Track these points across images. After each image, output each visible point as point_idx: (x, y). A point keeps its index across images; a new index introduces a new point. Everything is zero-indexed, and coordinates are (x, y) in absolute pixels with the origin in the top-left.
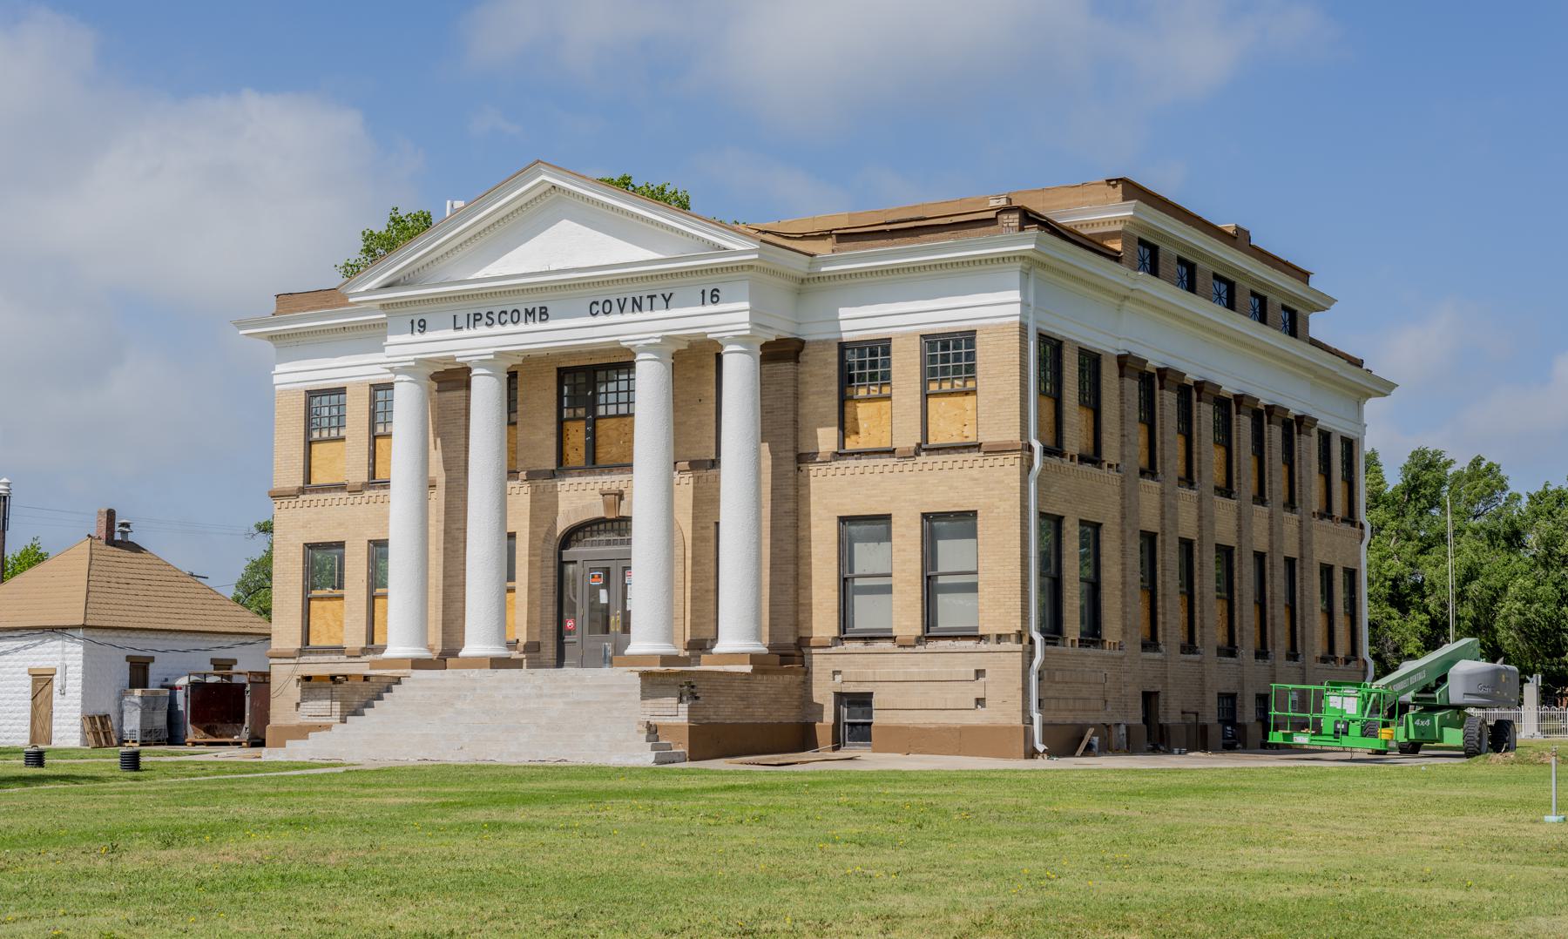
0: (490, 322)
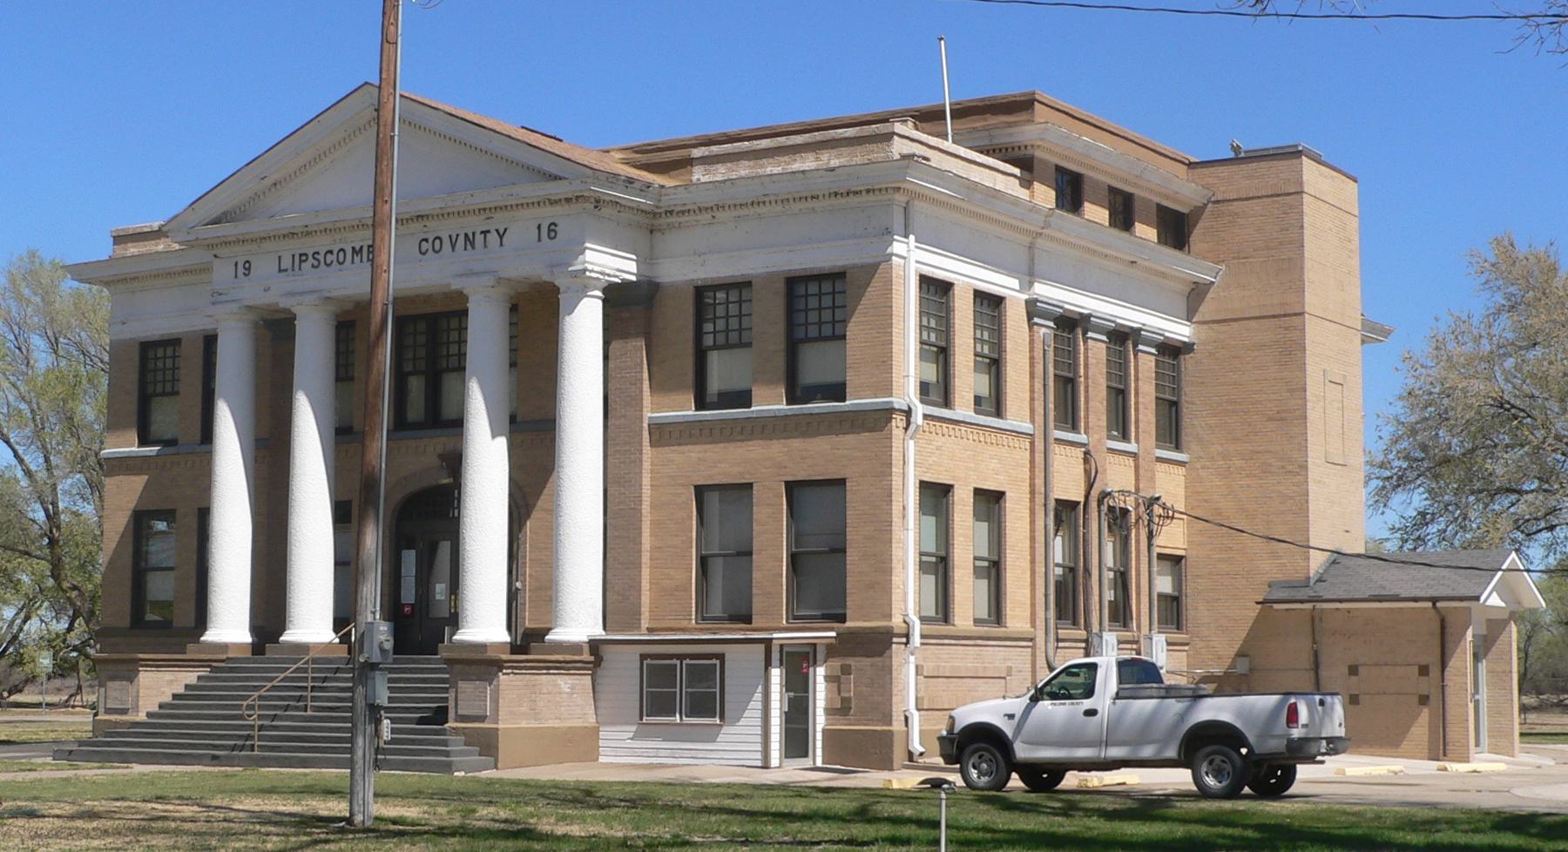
0: (316, 263)
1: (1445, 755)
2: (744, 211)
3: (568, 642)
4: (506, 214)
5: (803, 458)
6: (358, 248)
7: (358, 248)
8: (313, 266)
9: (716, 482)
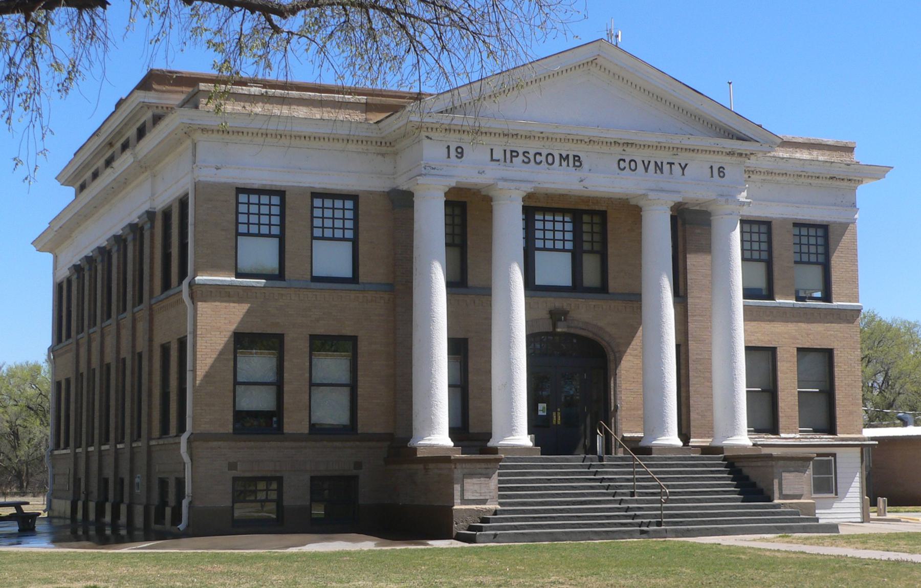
0: (526, 160)
2: (769, 177)
4: (691, 154)
5: (808, 335)
6: (564, 156)
7: (564, 156)
9: (754, 345)
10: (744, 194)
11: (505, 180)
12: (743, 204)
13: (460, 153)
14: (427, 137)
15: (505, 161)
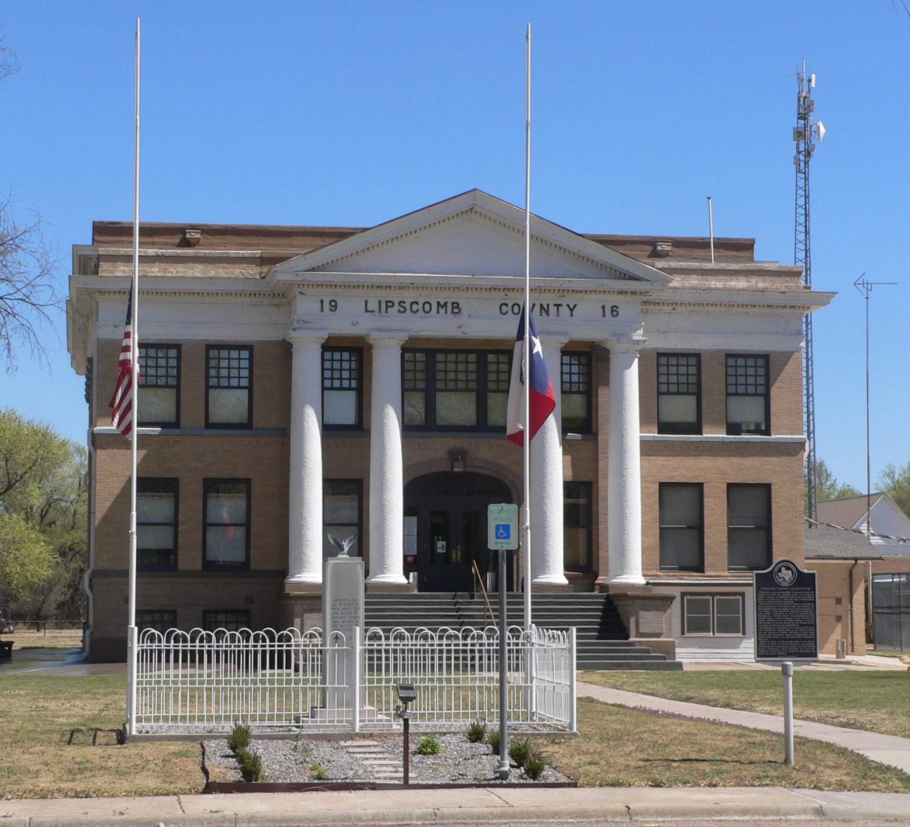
0: (402, 309)
1: (853, 651)
2: (696, 308)
3: (638, 584)
4: (579, 295)
6: (442, 303)
7: (442, 303)
8: (399, 311)
10: (641, 332)
11: (380, 330)
12: (638, 342)
13: (334, 306)
14: (301, 293)
15: (380, 311)
